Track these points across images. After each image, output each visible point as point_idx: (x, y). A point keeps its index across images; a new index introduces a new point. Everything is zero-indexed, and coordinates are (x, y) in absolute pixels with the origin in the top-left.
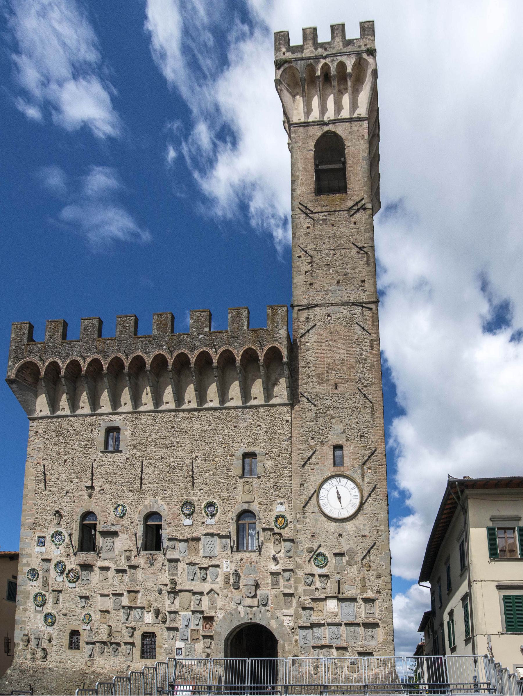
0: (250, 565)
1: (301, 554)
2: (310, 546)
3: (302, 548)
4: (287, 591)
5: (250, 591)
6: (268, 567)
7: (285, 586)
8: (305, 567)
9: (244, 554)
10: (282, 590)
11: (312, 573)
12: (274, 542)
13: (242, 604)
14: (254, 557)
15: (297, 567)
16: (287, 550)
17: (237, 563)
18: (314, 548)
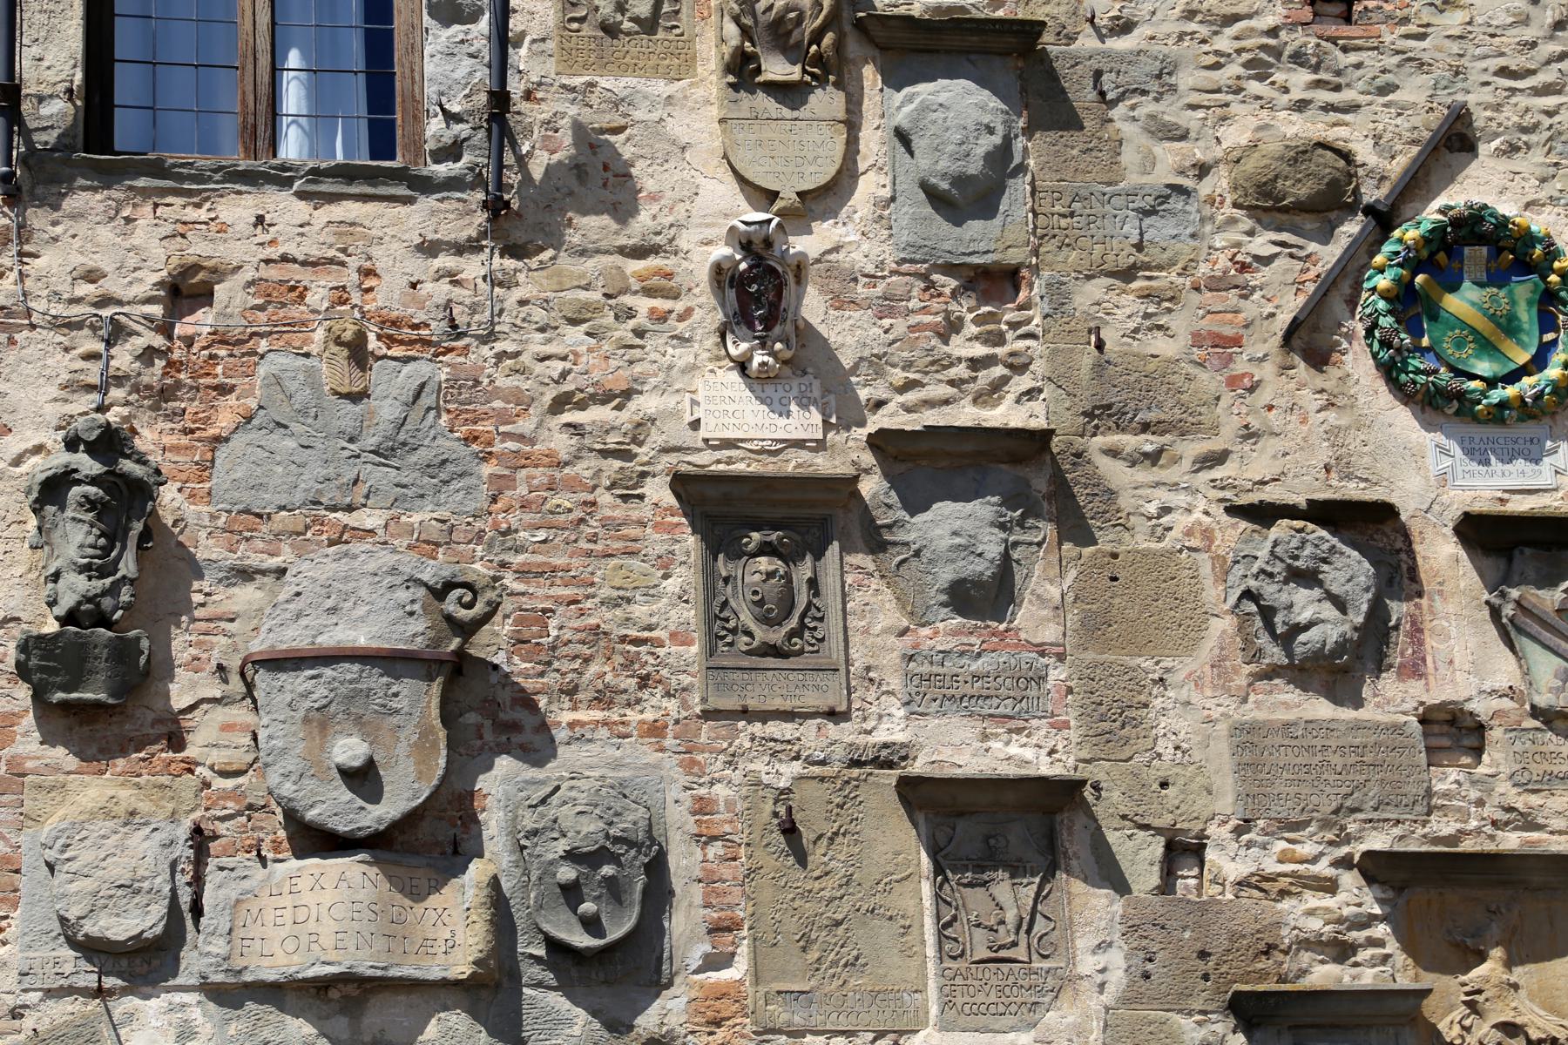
0: (334, 372)
1: (1160, 230)
2: (1299, 128)
3: (1168, 160)
4: (959, 749)
5: (349, 749)
6: (647, 404)
7: (931, 689)
8: (1230, 417)
9: (237, 209)
10: (892, 729)
11: (1353, 491)
12: (742, 71)
13: (201, 955)
14: (397, 266)
15: (1100, 415)
16: (934, 162)
17: (116, 333)
18: (1364, 152)
